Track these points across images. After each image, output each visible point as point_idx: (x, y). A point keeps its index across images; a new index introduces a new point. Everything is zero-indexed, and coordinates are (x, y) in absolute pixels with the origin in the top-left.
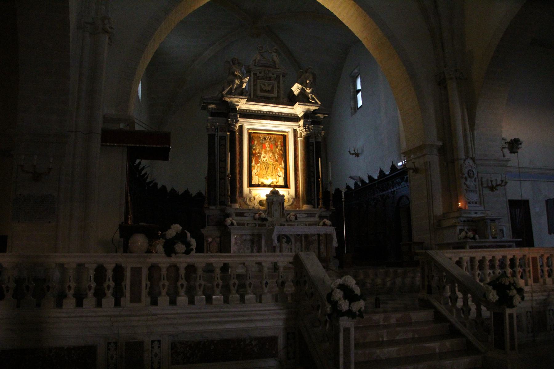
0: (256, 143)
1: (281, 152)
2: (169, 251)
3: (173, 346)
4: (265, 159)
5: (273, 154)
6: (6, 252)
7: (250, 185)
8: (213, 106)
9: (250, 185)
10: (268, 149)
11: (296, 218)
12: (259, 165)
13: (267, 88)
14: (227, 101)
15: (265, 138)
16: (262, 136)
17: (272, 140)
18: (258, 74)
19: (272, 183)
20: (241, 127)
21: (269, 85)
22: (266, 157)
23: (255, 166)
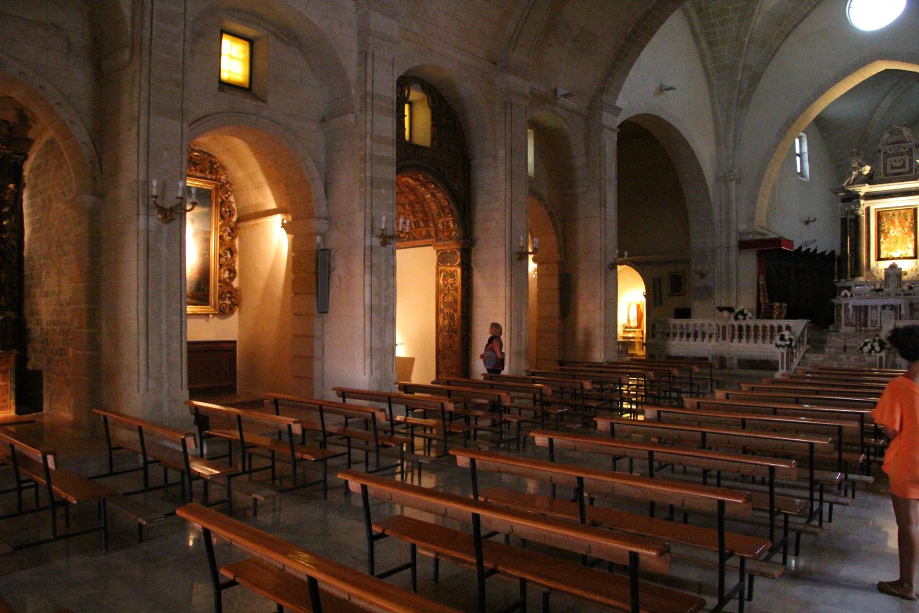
0: (884, 220)
1: (911, 225)
2: (736, 318)
3: (739, 360)
4: (894, 234)
5: (903, 228)
6: (689, 317)
7: (879, 259)
8: (843, 194)
9: (879, 259)
10: (897, 223)
11: (910, 288)
12: (888, 240)
13: (898, 165)
14: (849, 191)
15: (894, 215)
16: (891, 213)
17: (901, 215)
18: (889, 152)
19: (902, 255)
20: (868, 209)
21: (900, 160)
22: (895, 231)
23: (883, 243)
